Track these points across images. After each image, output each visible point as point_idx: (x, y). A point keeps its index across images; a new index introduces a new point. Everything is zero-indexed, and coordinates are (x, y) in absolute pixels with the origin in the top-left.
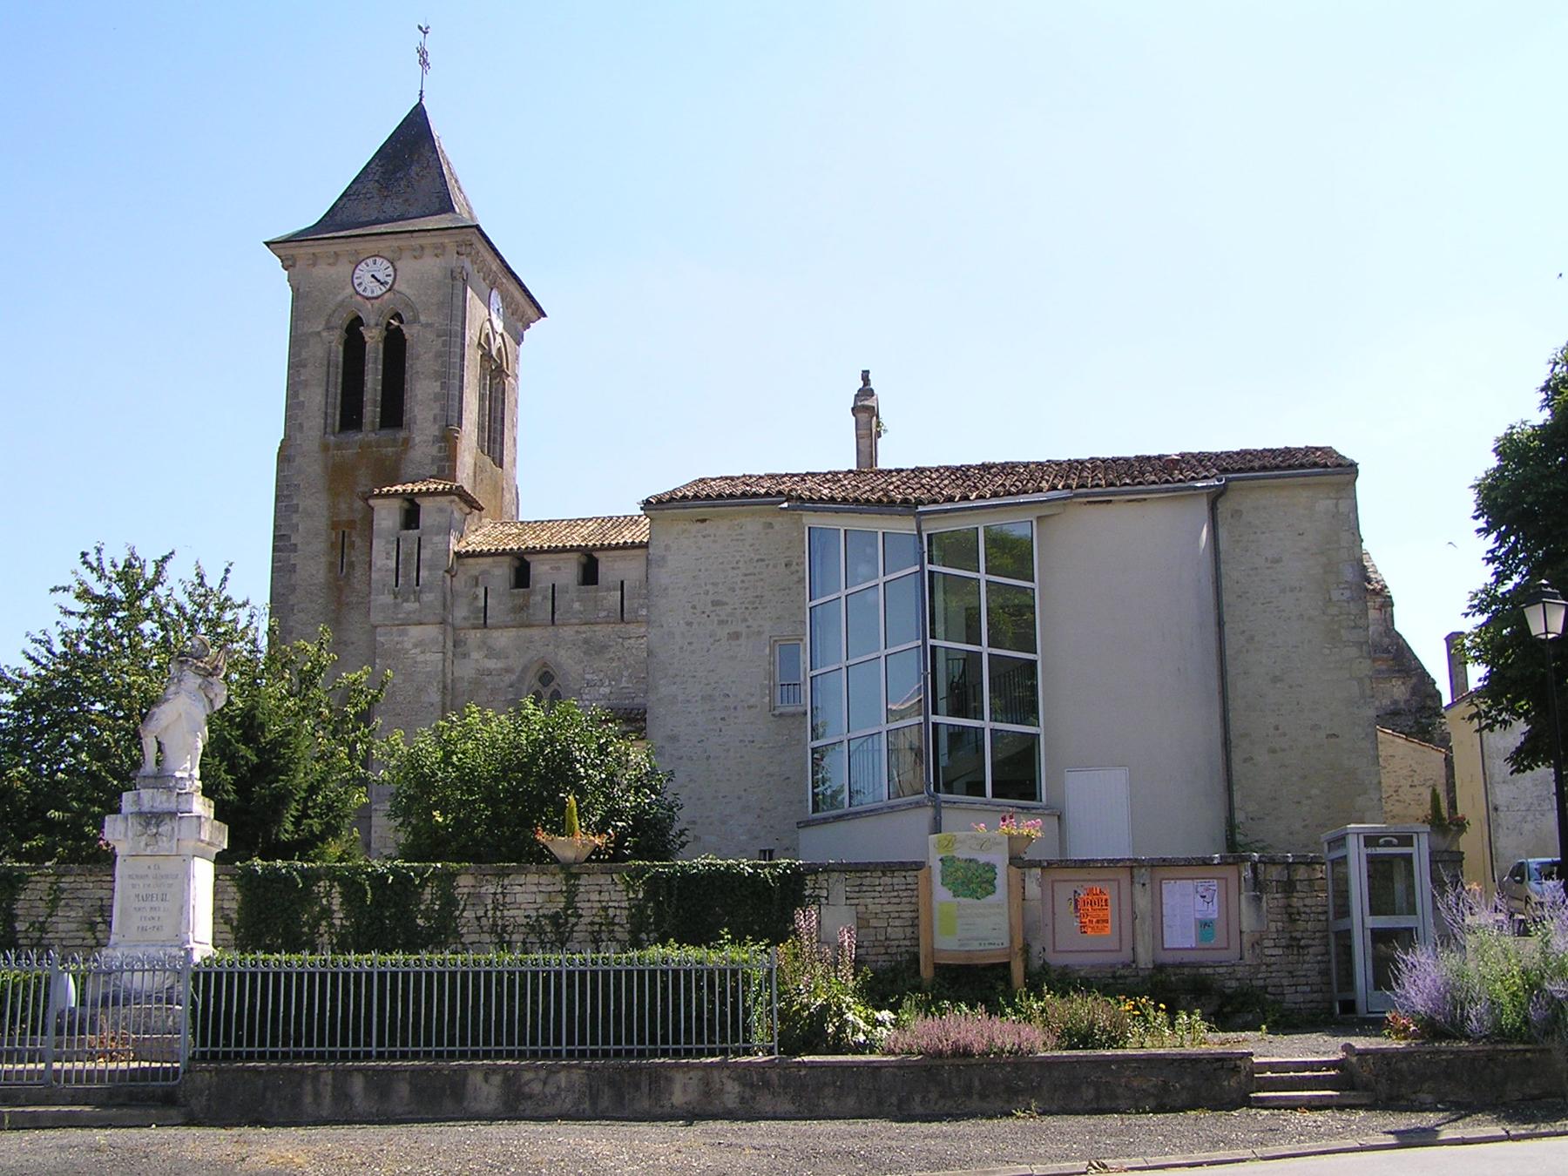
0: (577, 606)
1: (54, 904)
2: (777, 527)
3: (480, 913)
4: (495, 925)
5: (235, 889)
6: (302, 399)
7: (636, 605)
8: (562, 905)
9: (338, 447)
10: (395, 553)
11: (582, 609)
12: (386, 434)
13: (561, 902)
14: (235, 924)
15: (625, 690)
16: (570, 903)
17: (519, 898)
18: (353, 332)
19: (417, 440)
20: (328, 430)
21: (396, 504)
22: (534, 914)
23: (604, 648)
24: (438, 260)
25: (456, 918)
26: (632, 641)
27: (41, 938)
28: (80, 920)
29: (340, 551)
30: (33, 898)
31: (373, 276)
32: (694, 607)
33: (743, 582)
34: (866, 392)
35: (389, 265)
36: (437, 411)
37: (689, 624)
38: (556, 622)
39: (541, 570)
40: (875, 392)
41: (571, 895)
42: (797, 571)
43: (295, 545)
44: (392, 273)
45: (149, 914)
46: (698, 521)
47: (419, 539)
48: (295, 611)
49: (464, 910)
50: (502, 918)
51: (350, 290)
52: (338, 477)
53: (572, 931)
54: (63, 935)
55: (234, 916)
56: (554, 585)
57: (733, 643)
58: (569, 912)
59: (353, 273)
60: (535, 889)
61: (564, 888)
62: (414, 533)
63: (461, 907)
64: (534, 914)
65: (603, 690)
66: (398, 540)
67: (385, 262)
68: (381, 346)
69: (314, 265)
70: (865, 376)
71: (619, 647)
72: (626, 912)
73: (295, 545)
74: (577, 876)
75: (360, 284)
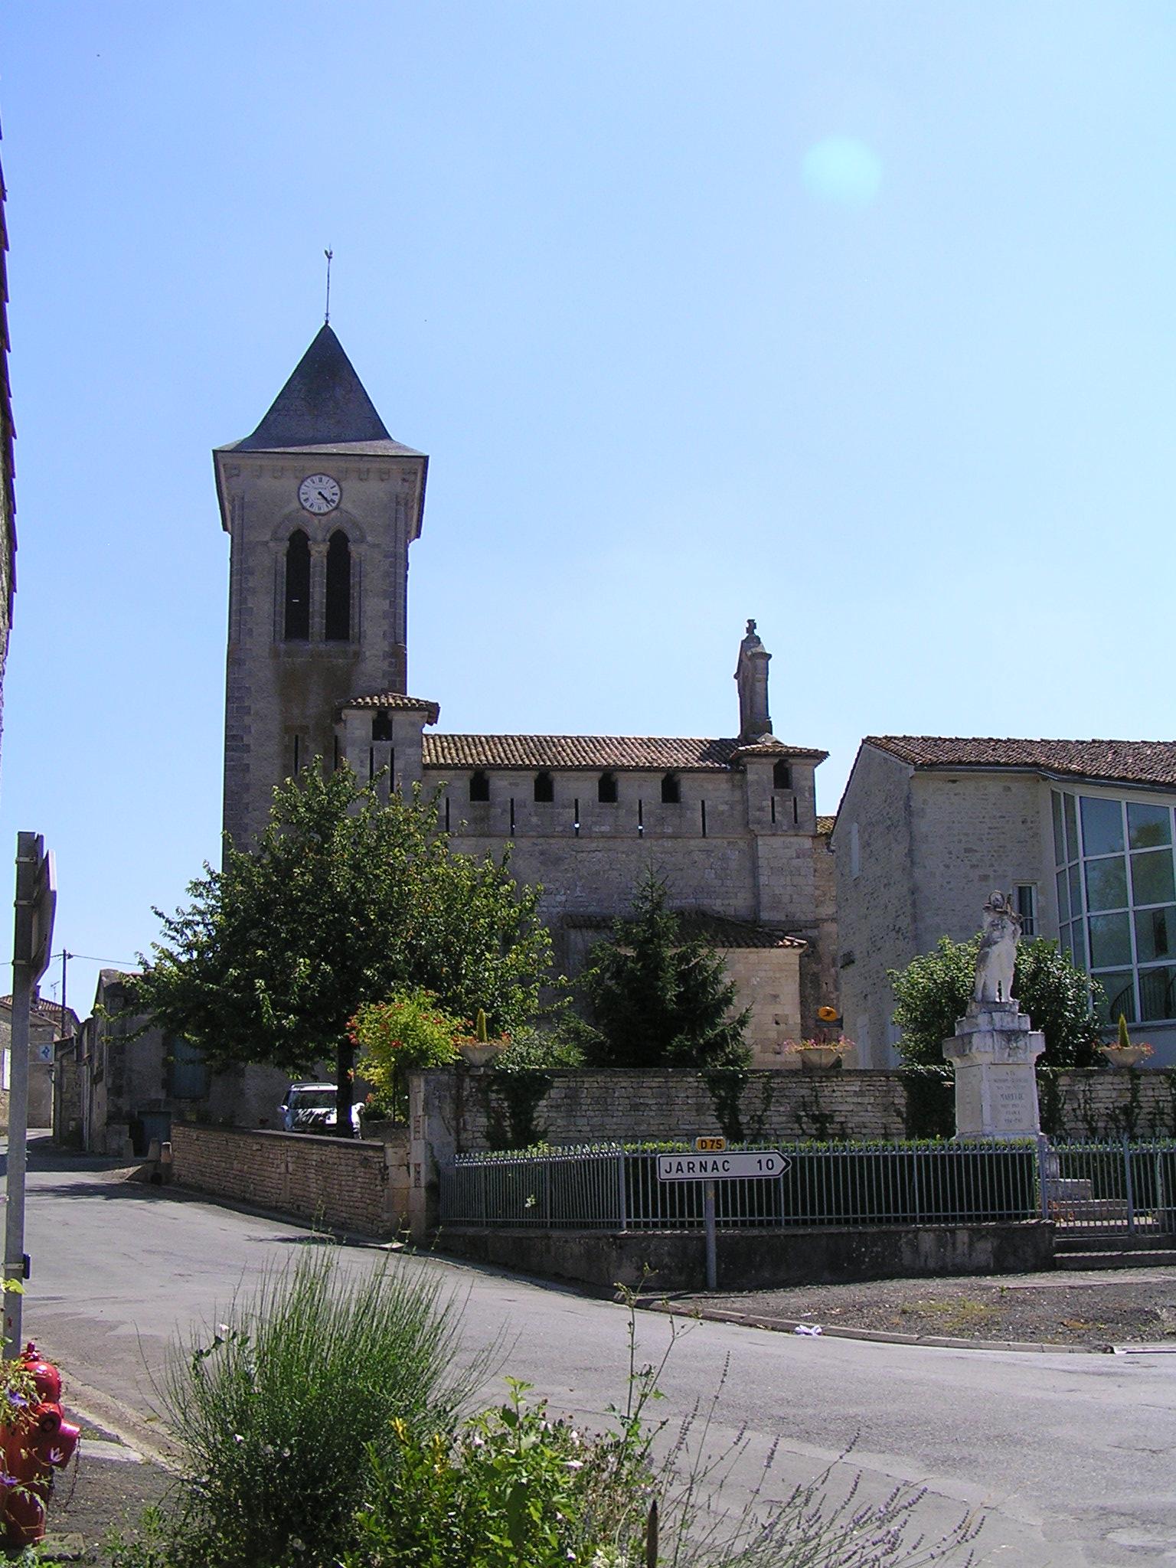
0: (534, 820)
1: (767, 1100)
2: (1014, 790)
3: (1076, 1106)
4: (1086, 1115)
5: (902, 1088)
6: (250, 605)
7: (590, 823)
8: (1129, 1099)
9: (288, 654)
10: (369, 762)
11: (539, 823)
12: (333, 646)
13: (1128, 1098)
14: (905, 1115)
15: (580, 899)
16: (1134, 1098)
17: (1101, 1094)
18: (299, 543)
19: (368, 654)
20: (277, 637)
21: (371, 715)
22: (1111, 1106)
23: (559, 860)
24: (383, 484)
25: (1059, 1109)
26: (584, 855)
27: (760, 1129)
28: (787, 1113)
29: (294, 755)
30: (750, 1095)
31: (320, 493)
32: (950, 853)
33: (989, 833)
34: (751, 640)
35: (335, 484)
36: (386, 628)
37: (947, 866)
38: (580, 835)
39: (499, 784)
40: (761, 640)
41: (1134, 1091)
42: (1032, 828)
43: (248, 746)
44: (338, 492)
45: (1012, 1110)
46: (950, 781)
47: (393, 750)
48: (250, 809)
49: (1064, 1103)
50: (1090, 1109)
51: (295, 505)
52: (290, 684)
53: (1136, 1119)
54: (777, 1126)
55: (903, 1109)
56: (512, 800)
57: (984, 883)
58: (1134, 1104)
59: (299, 489)
60: (1111, 1087)
61: (1130, 1086)
62: (386, 744)
63: (1062, 1101)
64: (1111, 1106)
65: (559, 898)
66: (372, 750)
67: (331, 481)
68: (325, 560)
69: (259, 477)
70: (752, 625)
71: (573, 858)
72: (1170, 1104)
73: (248, 746)
74: (1138, 1077)
75: (307, 500)
